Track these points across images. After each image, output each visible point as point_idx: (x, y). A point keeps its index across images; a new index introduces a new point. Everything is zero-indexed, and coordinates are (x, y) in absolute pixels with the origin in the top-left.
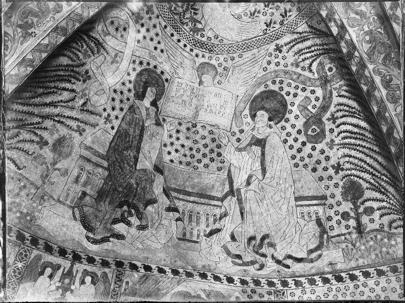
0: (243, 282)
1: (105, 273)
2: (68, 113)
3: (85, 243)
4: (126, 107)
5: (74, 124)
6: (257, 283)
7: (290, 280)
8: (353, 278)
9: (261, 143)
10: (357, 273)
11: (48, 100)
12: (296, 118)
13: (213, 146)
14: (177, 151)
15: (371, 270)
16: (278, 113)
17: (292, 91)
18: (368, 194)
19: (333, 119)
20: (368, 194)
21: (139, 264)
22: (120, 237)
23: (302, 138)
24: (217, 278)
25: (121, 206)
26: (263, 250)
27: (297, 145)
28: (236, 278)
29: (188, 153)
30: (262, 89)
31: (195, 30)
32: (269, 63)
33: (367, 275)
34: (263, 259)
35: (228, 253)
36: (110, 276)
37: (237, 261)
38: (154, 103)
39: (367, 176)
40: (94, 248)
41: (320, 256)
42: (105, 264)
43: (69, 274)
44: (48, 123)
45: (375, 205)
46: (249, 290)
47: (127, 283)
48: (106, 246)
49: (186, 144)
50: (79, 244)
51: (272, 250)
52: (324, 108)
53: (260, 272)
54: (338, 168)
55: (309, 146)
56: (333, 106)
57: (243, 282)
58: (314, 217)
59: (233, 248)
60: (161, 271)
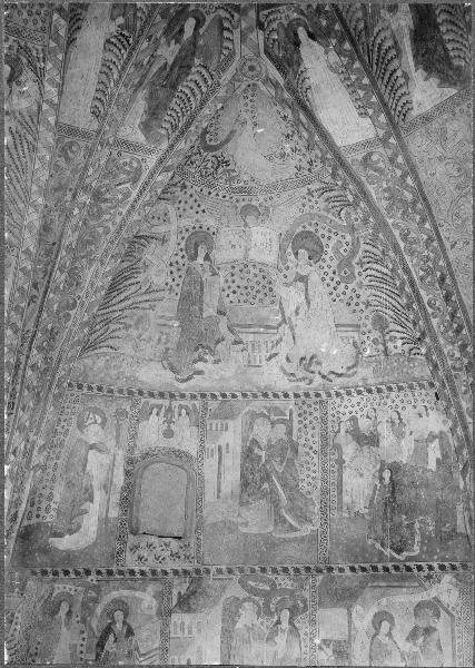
0: (296, 396)
2: (140, 299)
3: (176, 384)
4: (183, 273)
5: (147, 305)
6: (307, 395)
8: (379, 391)
9: (303, 279)
10: (383, 387)
11: (122, 297)
12: (330, 259)
13: (264, 282)
14: (234, 292)
15: (393, 386)
16: (316, 255)
17: (327, 235)
18: (392, 326)
19: (361, 263)
20: (392, 326)
21: (217, 394)
22: (200, 373)
23: (337, 279)
24: (276, 396)
25: (196, 349)
26: (312, 368)
27: (333, 284)
29: (244, 292)
30: (301, 229)
31: (230, 179)
32: (304, 205)
33: (390, 389)
34: (312, 375)
35: (285, 373)
38: (207, 258)
39: (392, 313)
40: (183, 386)
43: (169, 410)
44: (127, 312)
45: (398, 335)
48: (191, 382)
49: (241, 285)
50: (172, 385)
51: (319, 368)
52: (354, 253)
54: (368, 304)
55: (343, 285)
56: (360, 252)
57: (296, 396)
58: (351, 341)
59: (290, 368)
60: (234, 396)
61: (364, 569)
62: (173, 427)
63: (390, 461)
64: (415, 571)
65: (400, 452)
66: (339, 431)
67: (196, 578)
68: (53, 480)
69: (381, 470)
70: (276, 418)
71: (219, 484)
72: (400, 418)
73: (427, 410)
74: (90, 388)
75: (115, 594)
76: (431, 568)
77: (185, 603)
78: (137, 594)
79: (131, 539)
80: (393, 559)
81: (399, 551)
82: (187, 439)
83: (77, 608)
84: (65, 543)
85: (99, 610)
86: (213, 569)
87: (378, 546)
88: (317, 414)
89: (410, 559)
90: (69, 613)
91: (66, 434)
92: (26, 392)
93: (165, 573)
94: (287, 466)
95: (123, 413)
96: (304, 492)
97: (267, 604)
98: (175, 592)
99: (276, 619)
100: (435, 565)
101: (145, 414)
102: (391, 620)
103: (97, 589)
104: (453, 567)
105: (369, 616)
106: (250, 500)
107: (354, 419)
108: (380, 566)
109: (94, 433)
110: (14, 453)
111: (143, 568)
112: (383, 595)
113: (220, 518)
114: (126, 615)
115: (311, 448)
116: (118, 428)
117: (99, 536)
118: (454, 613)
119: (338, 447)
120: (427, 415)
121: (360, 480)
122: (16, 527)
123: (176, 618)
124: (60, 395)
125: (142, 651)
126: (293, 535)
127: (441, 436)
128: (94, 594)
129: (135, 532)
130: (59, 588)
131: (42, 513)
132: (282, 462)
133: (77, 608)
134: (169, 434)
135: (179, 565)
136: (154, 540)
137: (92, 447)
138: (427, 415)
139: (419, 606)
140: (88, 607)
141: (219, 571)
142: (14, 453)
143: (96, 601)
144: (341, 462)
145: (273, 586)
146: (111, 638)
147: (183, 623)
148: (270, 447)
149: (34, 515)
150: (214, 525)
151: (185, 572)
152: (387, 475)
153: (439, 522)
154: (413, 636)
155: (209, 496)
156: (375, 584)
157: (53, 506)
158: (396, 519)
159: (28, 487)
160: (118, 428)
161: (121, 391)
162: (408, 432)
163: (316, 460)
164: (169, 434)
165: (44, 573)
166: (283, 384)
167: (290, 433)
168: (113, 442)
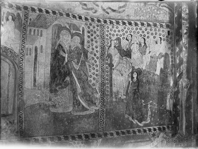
0: (86, 19)
1: (18, 13)
6: (93, 20)
7: (108, 20)
8: (136, 24)
10: (139, 23)
15: (145, 23)
24: (74, 17)
28: (83, 17)
33: (143, 24)
34: (97, 7)
36: (21, 15)
37: (85, 7)
41: (124, 11)
46: (88, 23)
47: (30, 19)
53: (94, 14)
60: (47, 12)
63: (136, 67)
65: (142, 63)
66: (110, 46)
69: (132, 73)
70: (74, 32)
71: (35, 75)
72: (145, 43)
73: (161, 40)
81: (140, 121)
87: (130, 119)
88: (98, 33)
89: (146, 125)
94: (81, 66)
106: (57, 88)
107: (118, 39)
108: (131, 130)
113: (37, 101)
115: (95, 55)
119: (110, 56)
120: (161, 43)
121: (122, 78)
126: (84, 113)
132: (78, 62)
144: (111, 65)
148: (70, 52)
150: (32, 107)
152: (135, 76)
162: (148, 52)
163: (98, 63)
167: (82, 43)
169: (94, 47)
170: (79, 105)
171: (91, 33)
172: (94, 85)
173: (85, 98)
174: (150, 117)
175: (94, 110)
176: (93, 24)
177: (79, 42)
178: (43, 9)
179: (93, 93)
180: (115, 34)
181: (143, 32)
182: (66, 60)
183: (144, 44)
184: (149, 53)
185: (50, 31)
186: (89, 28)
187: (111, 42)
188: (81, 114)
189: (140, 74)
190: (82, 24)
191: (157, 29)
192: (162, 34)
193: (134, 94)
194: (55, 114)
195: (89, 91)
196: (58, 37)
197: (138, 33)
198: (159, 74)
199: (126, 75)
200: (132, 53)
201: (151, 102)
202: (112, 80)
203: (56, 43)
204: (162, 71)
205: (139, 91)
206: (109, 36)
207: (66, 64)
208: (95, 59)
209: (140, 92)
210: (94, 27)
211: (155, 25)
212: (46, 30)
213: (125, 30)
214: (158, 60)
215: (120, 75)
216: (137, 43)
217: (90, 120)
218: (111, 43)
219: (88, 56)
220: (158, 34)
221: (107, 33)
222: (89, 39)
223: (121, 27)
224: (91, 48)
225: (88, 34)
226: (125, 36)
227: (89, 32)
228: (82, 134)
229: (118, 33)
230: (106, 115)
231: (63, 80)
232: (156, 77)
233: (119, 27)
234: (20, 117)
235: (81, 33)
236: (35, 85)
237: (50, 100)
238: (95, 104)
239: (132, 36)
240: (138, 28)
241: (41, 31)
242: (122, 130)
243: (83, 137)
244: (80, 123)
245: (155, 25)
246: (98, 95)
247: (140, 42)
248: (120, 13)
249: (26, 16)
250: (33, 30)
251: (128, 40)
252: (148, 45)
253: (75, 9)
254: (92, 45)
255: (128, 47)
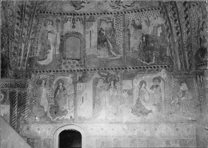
1: (81, 17)
6: (118, 13)
7: (126, 12)
15: (147, 9)
21: (89, 13)
22: (83, 7)
24: (108, 14)
26: (120, 4)
28: (113, 13)
33: (145, 10)
34: (120, 6)
35: (111, 6)
37: (114, 8)
40: (77, 11)
41: (134, 5)
42: (81, 15)
46: (116, 15)
47: (87, 19)
51: (122, 4)
53: (119, 10)
60: (94, 14)
61: (137, 68)
62: (75, 25)
63: (145, 34)
64: (153, 68)
65: (149, 31)
66: (129, 25)
67: (84, 72)
68: (38, 43)
69: (142, 37)
70: (108, 21)
71: (91, 42)
72: (149, 20)
74: (47, 13)
75: (59, 78)
76: (158, 67)
77: (81, 80)
78: (66, 77)
79: (63, 61)
80: (146, 65)
81: (148, 62)
82: (79, 28)
83: (48, 82)
84: (42, 63)
85: (54, 82)
86: (89, 69)
87: (141, 61)
88: (121, 19)
90: (45, 84)
91: (41, 27)
92: (26, 15)
93: (75, 71)
95: (58, 21)
96: (118, 44)
97: (107, 79)
98: (78, 77)
99: (110, 84)
100: (159, 66)
101: (66, 20)
102: (145, 83)
103: (53, 76)
104: (165, 67)
105: (139, 82)
106: (101, 47)
107: (133, 20)
108: (142, 67)
109: (49, 28)
110: (24, 35)
111: (67, 70)
112: (143, 76)
113: (91, 53)
114: (63, 84)
115: (120, 30)
116: (57, 25)
117: (53, 60)
118: (165, 81)
119: (128, 30)
120: (158, 18)
122: (27, 58)
123: (78, 84)
124: (37, 15)
125: (68, 95)
126: (114, 58)
127: (162, 25)
128: (52, 78)
129: (64, 59)
130: (42, 77)
131: (35, 53)
132: (110, 35)
133: (48, 82)
134: (74, 27)
135: (79, 68)
136: (71, 61)
137: (49, 32)
138: (158, 18)
139: (154, 79)
140: (51, 82)
141: (91, 70)
142: (24, 35)
143: (53, 80)
144: (129, 35)
145: (109, 74)
146: (59, 91)
147: (81, 86)
149: (32, 54)
150: (89, 56)
151: (81, 70)
152: (144, 38)
153: (161, 53)
154: (152, 88)
155: (88, 47)
156: (141, 73)
157: (38, 51)
158: (147, 52)
159: (29, 45)
160: (57, 25)
161: (57, 13)
162: (151, 24)
163: (121, 34)
164: (74, 27)
165: (37, 72)
166: (111, 10)
167: (113, 26)
168: (56, 30)
169: (119, 26)
170: (112, 54)
171: (118, 20)
172: (119, 45)
173: (114, 51)
174: (155, 60)
175: (120, 57)
176: (118, 15)
177: (111, 25)
178: (92, 13)
179: (118, 49)
180: (131, 18)
181: (146, 14)
182: (104, 35)
183: (148, 21)
184: (152, 25)
185: (96, 22)
186: (116, 17)
187: (129, 22)
188: (113, 58)
189: (147, 37)
190: (112, 17)
191: (154, 11)
192: (157, 13)
193: (144, 48)
194: (99, 59)
195: (117, 48)
196: (100, 24)
197: (144, 15)
198: (160, 36)
199: (138, 39)
200: (142, 26)
201: (155, 52)
202: (130, 42)
203: (99, 27)
204: (161, 34)
205: (147, 46)
206: (128, 19)
207: (104, 36)
208: (120, 32)
209: (148, 47)
210: (119, 17)
211: (142, 11)
212: (94, 22)
213: (137, 15)
214: (158, 28)
215: (135, 39)
216: (144, 21)
217: (117, 61)
218: (129, 23)
219: (116, 31)
220: (155, 14)
221: (126, 18)
222: (117, 23)
223: (134, 14)
224: (117, 27)
225: (116, 21)
226: (137, 18)
227: (116, 20)
228: (113, 68)
229: (133, 17)
230: (127, 59)
231: (103, 44)
232: (158, 38)
233: (133, 14)
234: (84, 60)
235: (112, 21)
236: (90, 47)
237: (97, 52)
238: (120, 54)
239: (140, 17)
240: (143, 12)
241: (92, 23)
242: (136, 67)
243: (114, 69)
244: (112, 63)
245: (152, 9)
246: (122, 50)
247: (146, 20)
248: (132, 7)
249: (85, 18)
250: (88, 24)
251: (139, 20)
252: (150, 21)
253: (109, 10)
254: (118, 26)
255: (139, 24)
